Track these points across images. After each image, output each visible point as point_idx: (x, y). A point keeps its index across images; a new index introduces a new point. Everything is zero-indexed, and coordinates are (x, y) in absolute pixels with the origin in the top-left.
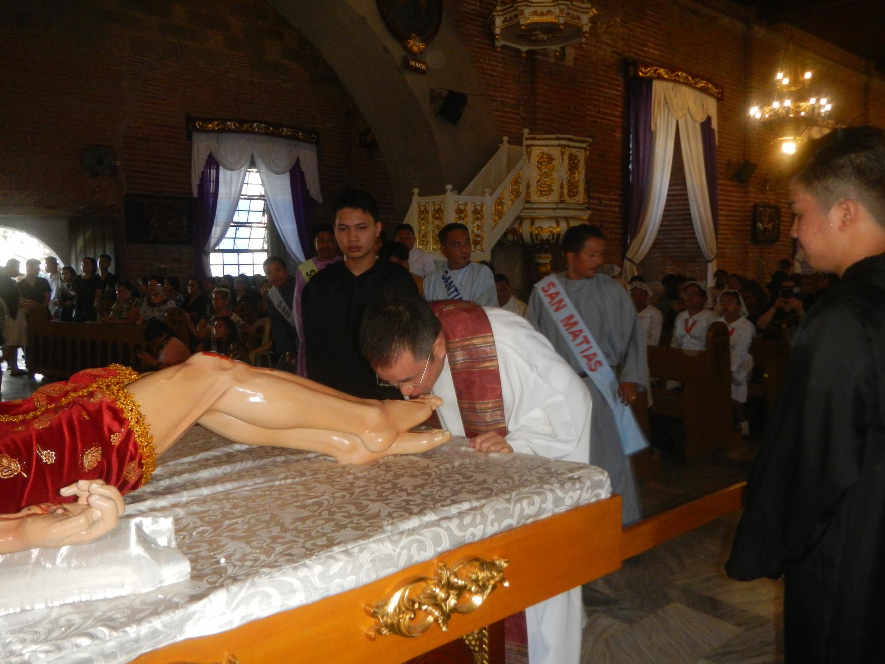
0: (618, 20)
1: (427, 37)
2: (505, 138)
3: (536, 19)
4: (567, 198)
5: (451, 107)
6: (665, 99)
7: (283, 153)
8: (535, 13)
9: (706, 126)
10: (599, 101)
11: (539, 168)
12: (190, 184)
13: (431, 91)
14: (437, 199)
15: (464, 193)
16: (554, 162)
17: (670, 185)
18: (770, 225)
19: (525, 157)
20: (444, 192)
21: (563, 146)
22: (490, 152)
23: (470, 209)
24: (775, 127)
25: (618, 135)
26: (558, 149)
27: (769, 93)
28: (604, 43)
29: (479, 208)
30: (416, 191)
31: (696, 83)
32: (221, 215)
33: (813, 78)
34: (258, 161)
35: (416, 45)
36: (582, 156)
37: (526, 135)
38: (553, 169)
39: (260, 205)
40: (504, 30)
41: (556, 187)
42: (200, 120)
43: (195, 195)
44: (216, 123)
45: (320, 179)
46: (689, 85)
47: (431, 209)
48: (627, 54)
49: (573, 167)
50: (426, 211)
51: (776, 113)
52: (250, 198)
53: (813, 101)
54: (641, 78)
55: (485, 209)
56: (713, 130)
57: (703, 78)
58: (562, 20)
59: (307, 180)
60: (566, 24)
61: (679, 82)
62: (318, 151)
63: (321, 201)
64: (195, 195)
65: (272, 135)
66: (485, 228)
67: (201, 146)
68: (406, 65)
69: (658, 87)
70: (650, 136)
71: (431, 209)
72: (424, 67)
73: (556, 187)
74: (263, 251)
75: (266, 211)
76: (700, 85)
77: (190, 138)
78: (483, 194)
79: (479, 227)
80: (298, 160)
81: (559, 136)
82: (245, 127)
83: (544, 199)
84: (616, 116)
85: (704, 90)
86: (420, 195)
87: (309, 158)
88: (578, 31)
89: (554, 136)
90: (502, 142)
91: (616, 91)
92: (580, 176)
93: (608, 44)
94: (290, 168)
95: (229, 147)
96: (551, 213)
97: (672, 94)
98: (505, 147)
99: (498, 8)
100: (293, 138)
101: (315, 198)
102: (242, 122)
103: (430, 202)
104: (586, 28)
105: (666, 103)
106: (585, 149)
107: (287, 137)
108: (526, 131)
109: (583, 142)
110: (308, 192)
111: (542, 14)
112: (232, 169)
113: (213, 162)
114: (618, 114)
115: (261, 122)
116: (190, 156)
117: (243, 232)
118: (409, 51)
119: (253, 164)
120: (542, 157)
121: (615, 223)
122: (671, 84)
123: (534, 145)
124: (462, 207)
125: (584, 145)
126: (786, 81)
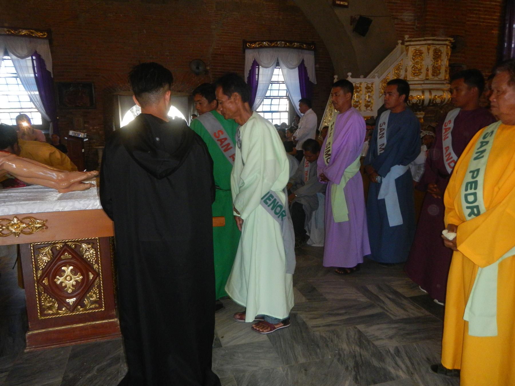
4: (430, 76)
5: (362, 26)
7: (294, 57)
10: (479, 10)
11: (413, 59)
13: (351, 17)
15: (368, 77)
16: (423, 55)
19: (405, 53)
21: (429, 45)
23: (363, 86)
25: (495, 32)
26: (426, 46)
29: (370, 85)
34: (281, 63)
36: (445, 51)
37: (406, 39)
38: (422, 60)
41: (424, 71)
42: (249, 42)
44: (257, 43)
49: (437, 56)
52: (278, 82)
55: (374, 86)
59: (308, 71)
62: (315, 54)
63: (316, 83)
65: (288, 47)
66: (374, 97)
67: (250, 56)
72: (346, 4)
73: (424, 71)
74: (286, 111)
75: (288, 91)
77: (244, 52)
79: (369, 97)
80: (303, 61)
81: (426, 38)
83: (416, 79)
84: (494, 19)
87: (309, 59)
89: (423, 39)
90: (397, 44)
92: (444, 62)
95: (265, 56)
96: (419, 87)
98: (399, 46)
100: (300, 48)
101: (312, 81)
102: (271, 42)
106: (447, 45)
109: (447, 40)
110: (308, 78)
113: (256, 64)
114: (495, 18)
117: (275, 101)
119: (278, 64)
120: (415, 52)
123: (410, 45)
125: (447, 43)
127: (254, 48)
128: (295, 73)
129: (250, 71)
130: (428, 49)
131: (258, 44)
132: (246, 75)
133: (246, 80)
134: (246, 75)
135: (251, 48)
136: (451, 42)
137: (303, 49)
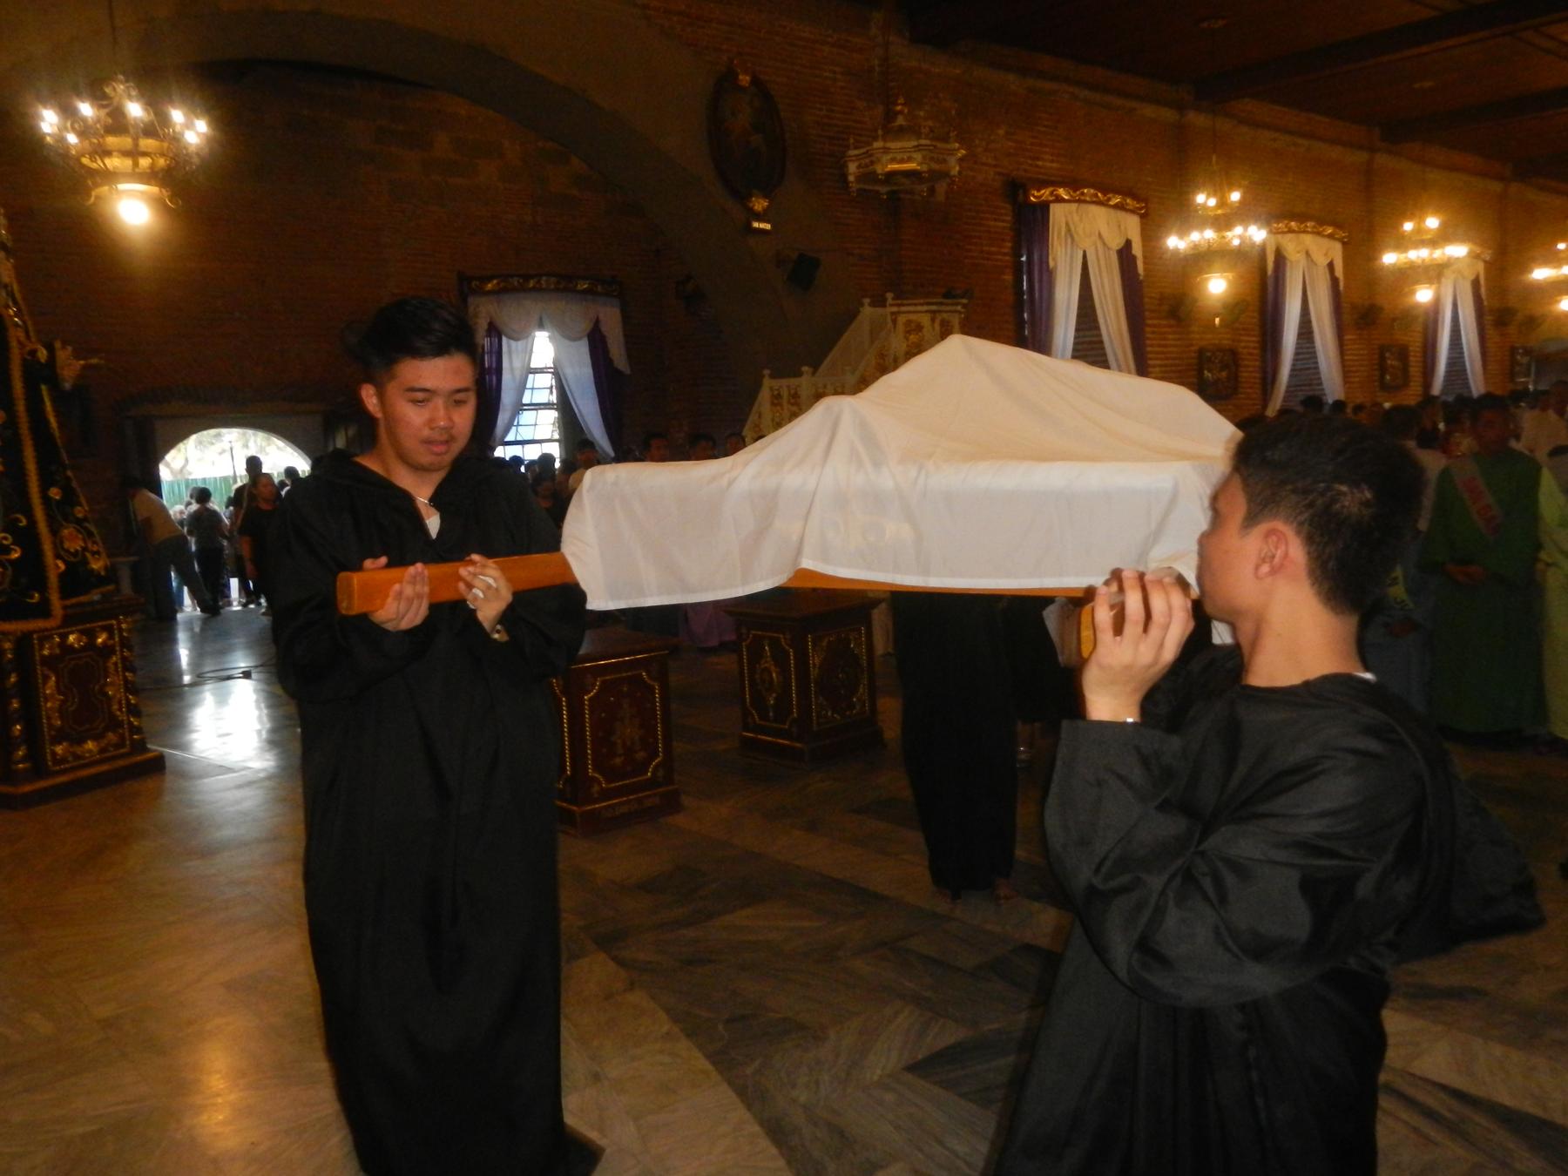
0: (1001, 132)
2: (867, 301)
3: (896, 166)
5: (803, 271)
6: (1067, 224)
8: (893, 160)
9: (1125, 253)
14: (793, 381)
17: (1077, 330)
18: (1224, 374)
20: (799, 374)
21: (934, 312)
22: (852, 315)
24: (1201, 259)
27: (1186, 217)
30: (767, 372)
32: (507, 398)
33: (1243, 202)
34: (546, 322)
35: (760, 204)
37: (890, 301)
39: (547, 380)
40: (859, 179)
45: (627, 343)
47: (785, 394)
50: (779, 396)
51: (1196, 246)
53: (1238, 230)
54: (1034, 205)
56: (1134, 258)
57: (1117, 192)
58: (925, 168)
60: (930, 171)
61: (1085, 202)
65: (566, 290)
68: (750, 224)
69: (1058, 213)
70: (1048, 276)
71: (785, 394)
72: (768, 227)
77: (465, 301)
80: (597, 322)
82: (531, 284)
85: (1120, 207)
86: (772, 376)
87: (611, 318)
88: (945, 175)
90: (862, 305)
91: (1003, 222)
97: (1076, 218)
98: (867, 311)
102: (527, 278)
103: (784, 384)
104: (955, 170)
105: (1069, 230)
108: (889, 296)
110: (611, 361)
111: (902, 161)
112: (516, 339)
113: (495, 331)
115: (548, 275)
118: (751, 211)
119: (541, 326)
122: (1074, 206)
126: (1212, 202)
128: (582, 350)
136: (964, 306)
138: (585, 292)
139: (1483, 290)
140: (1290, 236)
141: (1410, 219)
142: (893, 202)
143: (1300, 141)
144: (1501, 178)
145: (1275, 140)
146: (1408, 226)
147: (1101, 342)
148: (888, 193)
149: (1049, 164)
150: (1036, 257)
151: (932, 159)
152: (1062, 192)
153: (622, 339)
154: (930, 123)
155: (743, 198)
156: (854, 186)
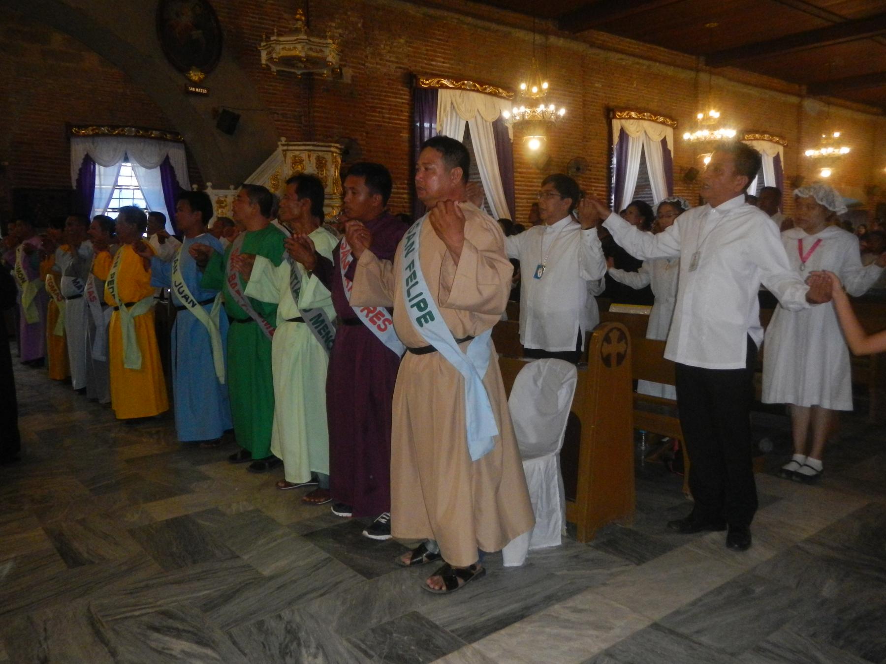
0: (402, 41)
1: (207, 67)
5: (228, 122)
6: (452, 103)
7: (155, 152)
10: (383, 108)
12: (70, 178)
21: (310, 151)
24: (524, 126)
25: (405, 135)
26: (307, 153)
28: (389, 61)
31: (485, 89)
33: (550, 88)
34: (131, 158)
35: (195, 75)
42: (75, 126)
43: (75, 188)
44: (90, 128)
46: (478, 91)
48: (413, 68)
53: (542, 108)
56: (507, 128)
64: (75, 188)
65: (142, 136)
72: (205, 91)
76: (488, 90)
78: (228, 188)
84: (402, 120)
87: (178, 157)
91: (403, 97)
93: (392, 62)
94: (160, 163)
95: (102, 148)
97: (459, 100)
99: (263, 44)
100: (161, 139)
106: (333, 152)
107: (156, 138)
110: (178, 183)
111: (290, 50)
112: (105, 166)
115: (132, 126)
116: (69, 156)
118: (189, 79)
119: (126, 160)
121: (403, 207)
122: (458, 92)
124: (222, 199)
125: (333, 149)
127: (84, 136)
128: (156, 173)
129: (80, 170)
130: (309, 156)
131: (92, 130)
132: (74, 176)
133: (74, 185)
134: (74, 176)
135: (79, 136)
137: (166, 140)
138: (156, 138)
139: (782, 164)
140: (632, 121)
141: (702, 111)
142: (306, 80)
143: (641, 61)
144: (799, 95)
145: (622, 59)
146: (700, 116)
147: (481, 182)
148: (301, 74)
149: (439, 63)
150: (427, 125)
151: (311, 49)
152: (445, 82)
153: (185, 169)
154: (340, 31)
155: (183, 70)
156: (274, 68)
